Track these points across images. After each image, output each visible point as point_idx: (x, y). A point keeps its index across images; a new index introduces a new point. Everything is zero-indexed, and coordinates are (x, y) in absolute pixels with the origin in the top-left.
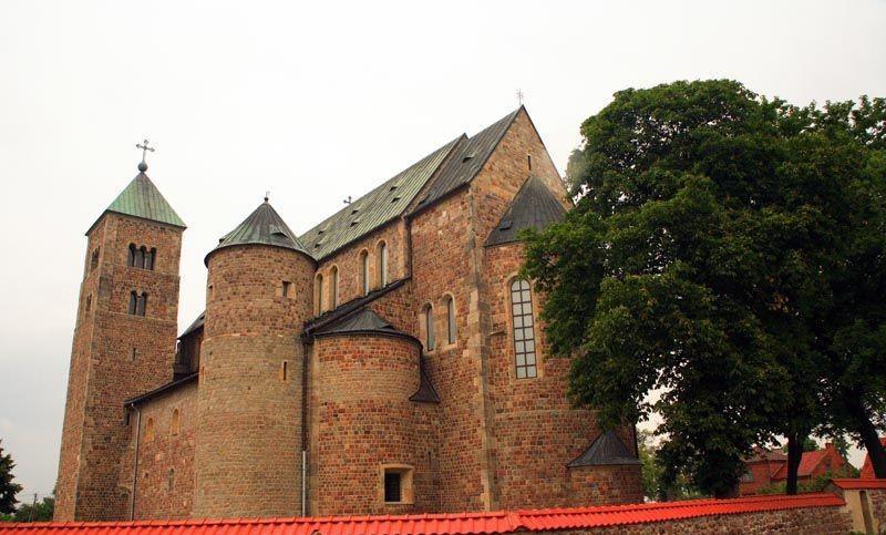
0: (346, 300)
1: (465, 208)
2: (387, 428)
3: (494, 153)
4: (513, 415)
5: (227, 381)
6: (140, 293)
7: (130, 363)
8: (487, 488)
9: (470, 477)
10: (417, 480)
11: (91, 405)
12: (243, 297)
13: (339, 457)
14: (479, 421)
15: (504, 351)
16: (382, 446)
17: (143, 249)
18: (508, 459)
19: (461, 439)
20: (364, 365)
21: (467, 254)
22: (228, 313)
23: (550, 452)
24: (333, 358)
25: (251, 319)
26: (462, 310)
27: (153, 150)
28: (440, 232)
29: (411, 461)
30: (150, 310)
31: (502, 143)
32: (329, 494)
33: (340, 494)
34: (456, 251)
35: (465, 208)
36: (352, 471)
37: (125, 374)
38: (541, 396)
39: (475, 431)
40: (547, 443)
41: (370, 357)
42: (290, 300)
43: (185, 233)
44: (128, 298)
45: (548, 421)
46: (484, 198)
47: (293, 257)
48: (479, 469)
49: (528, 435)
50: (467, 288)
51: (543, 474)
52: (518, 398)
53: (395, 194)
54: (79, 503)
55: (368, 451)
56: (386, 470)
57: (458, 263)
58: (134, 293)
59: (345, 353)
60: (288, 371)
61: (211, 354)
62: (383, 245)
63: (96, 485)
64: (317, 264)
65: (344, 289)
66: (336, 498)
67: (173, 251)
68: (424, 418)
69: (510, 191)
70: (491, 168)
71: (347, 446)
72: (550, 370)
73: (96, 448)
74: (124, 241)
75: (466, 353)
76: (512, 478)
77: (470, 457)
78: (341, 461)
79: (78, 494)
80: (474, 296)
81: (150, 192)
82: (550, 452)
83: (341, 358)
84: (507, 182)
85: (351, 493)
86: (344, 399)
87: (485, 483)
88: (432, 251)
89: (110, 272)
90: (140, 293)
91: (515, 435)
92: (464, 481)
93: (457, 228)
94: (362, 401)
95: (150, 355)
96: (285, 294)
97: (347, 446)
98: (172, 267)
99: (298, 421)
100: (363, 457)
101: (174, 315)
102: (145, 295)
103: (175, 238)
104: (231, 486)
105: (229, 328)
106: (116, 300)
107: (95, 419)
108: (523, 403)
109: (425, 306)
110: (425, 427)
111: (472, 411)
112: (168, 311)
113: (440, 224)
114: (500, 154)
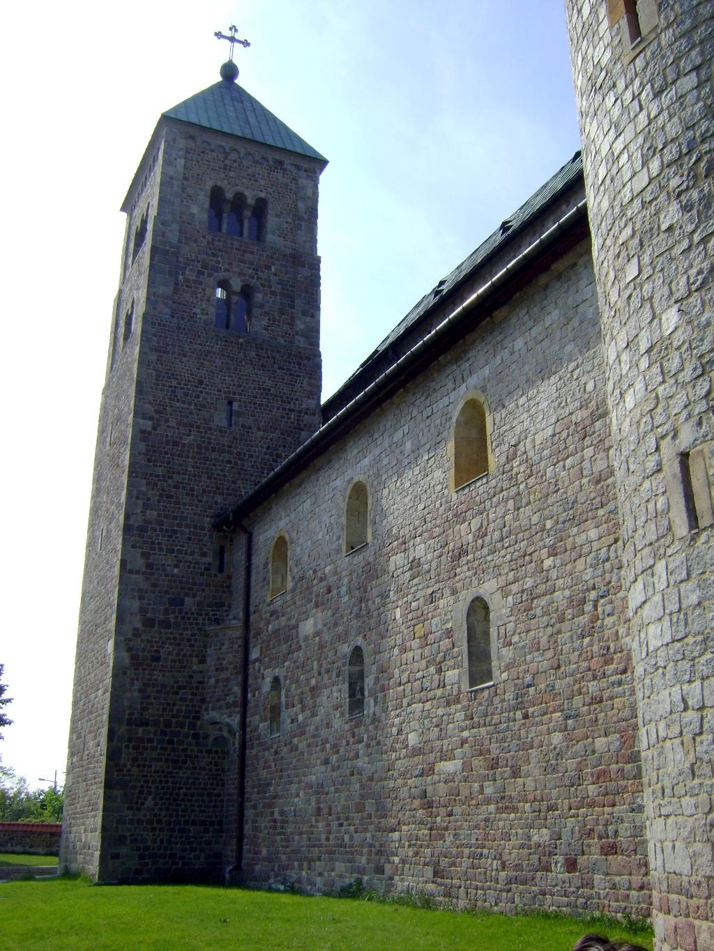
11: (137, 521)
17: (240, 197)
27: (246, 44)
37: (214, 455)
54: (113, 755)
67: (301, 205)
73: (149, 623)
89: (173, 237)
98: (301, 236)
103: (303, 181)
106: (187, 297)
112: (300, 326)
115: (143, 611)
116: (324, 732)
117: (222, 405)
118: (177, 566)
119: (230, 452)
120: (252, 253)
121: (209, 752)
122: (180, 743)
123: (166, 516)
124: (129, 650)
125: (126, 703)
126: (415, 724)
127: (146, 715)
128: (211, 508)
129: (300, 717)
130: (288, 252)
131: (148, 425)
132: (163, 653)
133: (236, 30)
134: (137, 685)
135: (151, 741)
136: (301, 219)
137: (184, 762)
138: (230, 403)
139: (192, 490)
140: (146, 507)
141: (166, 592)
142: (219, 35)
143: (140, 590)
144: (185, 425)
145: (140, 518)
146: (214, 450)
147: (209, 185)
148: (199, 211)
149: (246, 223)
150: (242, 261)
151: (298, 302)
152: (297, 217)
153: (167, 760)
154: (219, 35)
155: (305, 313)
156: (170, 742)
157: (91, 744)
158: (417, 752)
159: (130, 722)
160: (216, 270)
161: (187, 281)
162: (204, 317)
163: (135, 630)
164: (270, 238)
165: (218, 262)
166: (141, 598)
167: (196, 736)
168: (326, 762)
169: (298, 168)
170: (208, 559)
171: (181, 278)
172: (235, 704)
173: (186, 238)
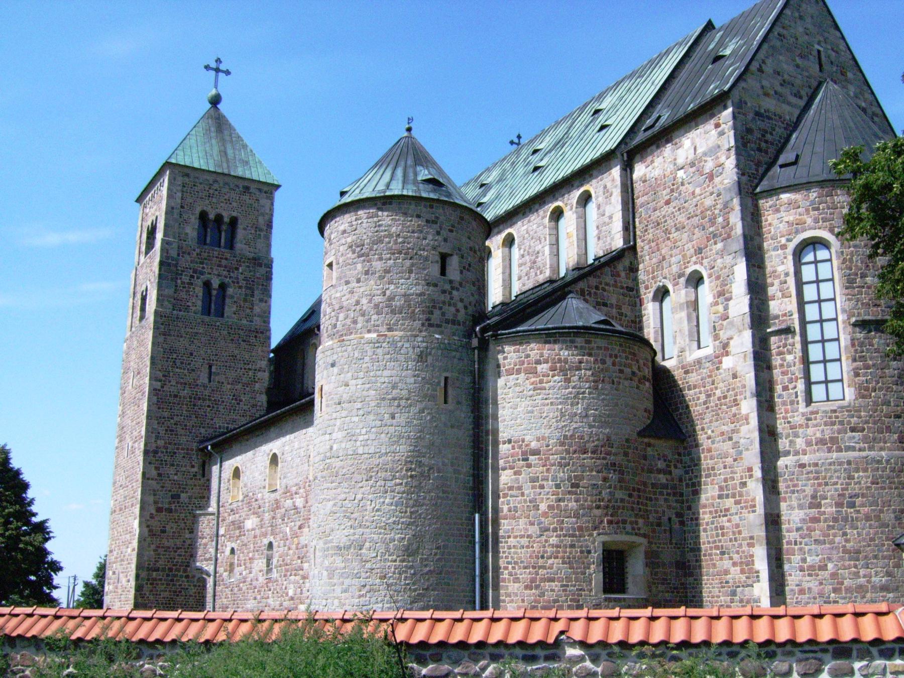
0: (530, 285)
1: (722, 134)
2: (605, 479)
3: (765, 46)
4: (805, 459)
5: (359, 405)
6: (216, 283)
7: (205, 386)
8: (764, 575)
9: (736, 557)
10: (652, 560)
11: (153, 447)
12: (381, 278)
13: (532, 524)
14: (750, 469)
15: (789, 358)
16: (598, 507)
17: (219, 218)
18: (798, 529)
19: (720, 497)
20: (568, 380)
21: (726, 206)
22: (358, 303)
23: (868, 518)
24: (519, 372)
25: (393, 312)
26: (721, 294)
27: (228, 73)
28: (681, 174)
29: (642, 532)
30: (230, 309)
31: (777, 30)
32: (516, 580)
33: (533, 580)
34: (709, 202)
35: (722, 134)
36: (553, 546)
37: (199, 403)
38: (853, 430)
39: (744, 484)
40: (863, 505)
41: (579, 369)
42: (451, 282)
43: (278, 195)
44: (199, 291)
45: (865, 470)
46: (751, 116)
47: (454, 216)
48: (751, 545)
49: (831, 492)
50: (728, 259)
51: (855, 554)
52: (814, 433)
53: (601, 119)
55: (577, 516)
56: (604, 543)
57: (713, 221)
58: (207, 285)
59: (538, 362)
60: (450, 391)
61: (333, 365)
62: (586, 198)
63: (161, 563)
64: (490, 228)
65: (525, 269)
66: (526, 587)
67: (261, 219)
68: (661, 464)
69: (789, 104)
70: (760, 70)
71: (543, 507)
72: (867, 389)
73: (159, 510)
74: (191, 207)
75: (727, 362)
76: (804, 560)
77: (737, 526)
78: (534, 530)
79: (137, 576)
80: (741, 271)
81: (226, 132)
82: (868, 518)
83: (534, 372)
84: (785, 91)
85: (552, 580)
86: (539, 433)
87: (762, 565)
88: (668, 203)
89: (173, 253)
90: (216, 283)
91: (809, 490)
92: (726, 564)
93: (709, 166)
94: (565, 437)
95: (232, 375)
96: (443, 272)
97: (543, 507)
98: (260, 244)
99: (466, 467)
100: (569, 522)
101: (266, 316)
102: (223, 287)
103: (263, 201)
104: (368, 565)
105: (359, 326)
106: (183, 295)
107: (157, 468)
108: (821, 442)
109: (658, 290)
110: (663, 478)
111: (741, 453)
112: (257, 309)
113: (680, 161)
114: (773, 47)
115: (155, 502)
116: (254, 583)
117: (205, 370)
118: (176, 474)
119: (210, 400)
120: (226, 259)
121: (195, 586)
122: (178, 580)
123: (170, 444)
124: (148, 526)
125: (146, 558)
126: (292, 586)
127: (158, 565)
128: (197, 437)
129: (244, 573)
130: (251, 255)
131: (158, 385)
132: (168, 528)
133: (221, 62)
134: (153, 547)
135: (161, 580)
136: (261, 230)
137: (180, 592)
138: (210, 367)
139: (186, 426)
140: (157, 437)
141: (170, 491)
142: (207, 67)
143: (154, 490)
144: (181, 383)
145: (154, 445)
146: (199, 399)
147: (198, 210)
148: (191, 231)
149: (223, 234)
150: (219, 266)
151: (256, 292)
152: (257, 228)
153: (170, 591)
154: (207, 67)
155: (261, 300)
156: (172, 580)
157: (124, 580)
158: (292, 599)
159: (148, 569)
160: (202, 273)
161: (183, 283)
162: (194, 308)
163: (151, 514)
164: (239, 246)
165: (203, 268)
166: (155, 495)
167: (187, 577)
168: (255, 598)
169: (260, 190)
170: (195, 469)
171: (179, 281)
172: (210, 559)
173: (183, 253)
